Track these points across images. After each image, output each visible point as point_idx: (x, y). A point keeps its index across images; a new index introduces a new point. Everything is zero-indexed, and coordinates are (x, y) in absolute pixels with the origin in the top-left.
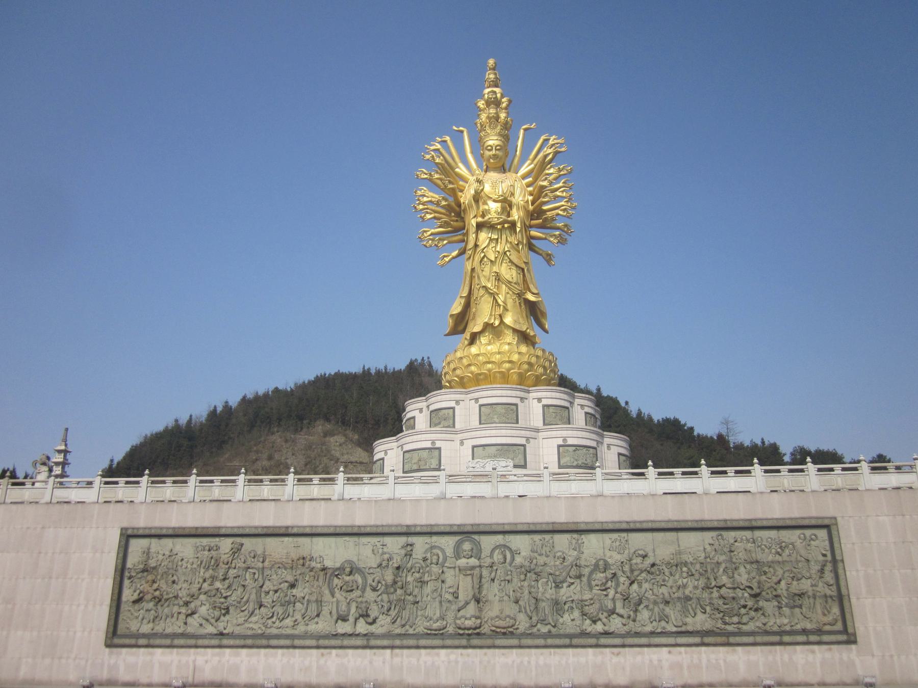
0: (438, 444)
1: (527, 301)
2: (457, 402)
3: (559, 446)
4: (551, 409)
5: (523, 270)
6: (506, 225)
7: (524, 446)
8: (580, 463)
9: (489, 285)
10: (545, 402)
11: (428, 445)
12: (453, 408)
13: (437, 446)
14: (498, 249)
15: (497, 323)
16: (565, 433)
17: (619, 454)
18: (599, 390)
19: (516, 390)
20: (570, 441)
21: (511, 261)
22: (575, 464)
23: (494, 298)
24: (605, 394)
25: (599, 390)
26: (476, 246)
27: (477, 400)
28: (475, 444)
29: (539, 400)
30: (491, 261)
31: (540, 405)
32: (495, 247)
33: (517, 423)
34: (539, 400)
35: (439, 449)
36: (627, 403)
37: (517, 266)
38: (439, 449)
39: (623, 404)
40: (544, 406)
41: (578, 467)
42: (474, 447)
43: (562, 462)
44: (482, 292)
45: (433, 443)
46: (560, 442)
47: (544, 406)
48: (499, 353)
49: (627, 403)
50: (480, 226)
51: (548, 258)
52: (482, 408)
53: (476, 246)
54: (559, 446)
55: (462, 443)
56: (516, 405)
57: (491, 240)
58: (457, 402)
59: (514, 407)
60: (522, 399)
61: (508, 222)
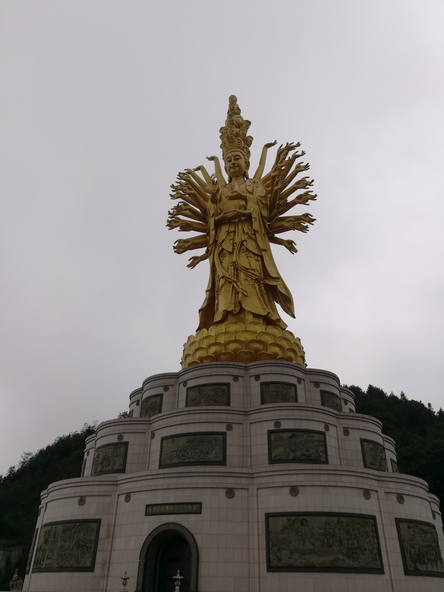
0: (126, 439)
1: (267, 287)
2: (166, 388)
3: (270, 433)
4: (272, 388)
5: (262, 257)
6: (243, 218)
7: (224, 434)
8: (298, 454)
9: (227, 275)
10: (264, 379)
11: (114, 439)
12: (161, 396)
13: (124, 440)
14: (236, 241)
15: (237, 309)
16: (277, 415)
17: (363, 441)
18: (403, 395)
19: (227, 366)
20: (285, 425)
21: (248, 250)
22: (291, 456)
23: (233, 286)
24: (409, 398)
25: (403, 395)
26: (215, 241)
27: (185, 383)
28: (164, 435)
29: (257, 377)
30: (230, 253)
31: (258, 383)
32: (233, 239)
33: (228, 404)
34: (257, 377)
35: (126, 444)
36: (429, 405)
37: (255, 254)
38: (126, 444)
39: (427, 406)
40: (262, 384)
41: (295, 460)
42: (163, 439)
43: (273, 454)
44: (222, 281)
45: (120, 437)
46: (271, 426)
47: (262, 384)
48: (226, 333)
49: (429, 405)
50: (218, 225)
51: (290, 246)
52: (190, 393)
53: (215, 241)
54: (270, 433)
55: (153, 436)
56: (228, 385)
57: (228, 233)
58: (166, 388)
59: (226, 388)
60: (236, 378)
61: (244, 215)
